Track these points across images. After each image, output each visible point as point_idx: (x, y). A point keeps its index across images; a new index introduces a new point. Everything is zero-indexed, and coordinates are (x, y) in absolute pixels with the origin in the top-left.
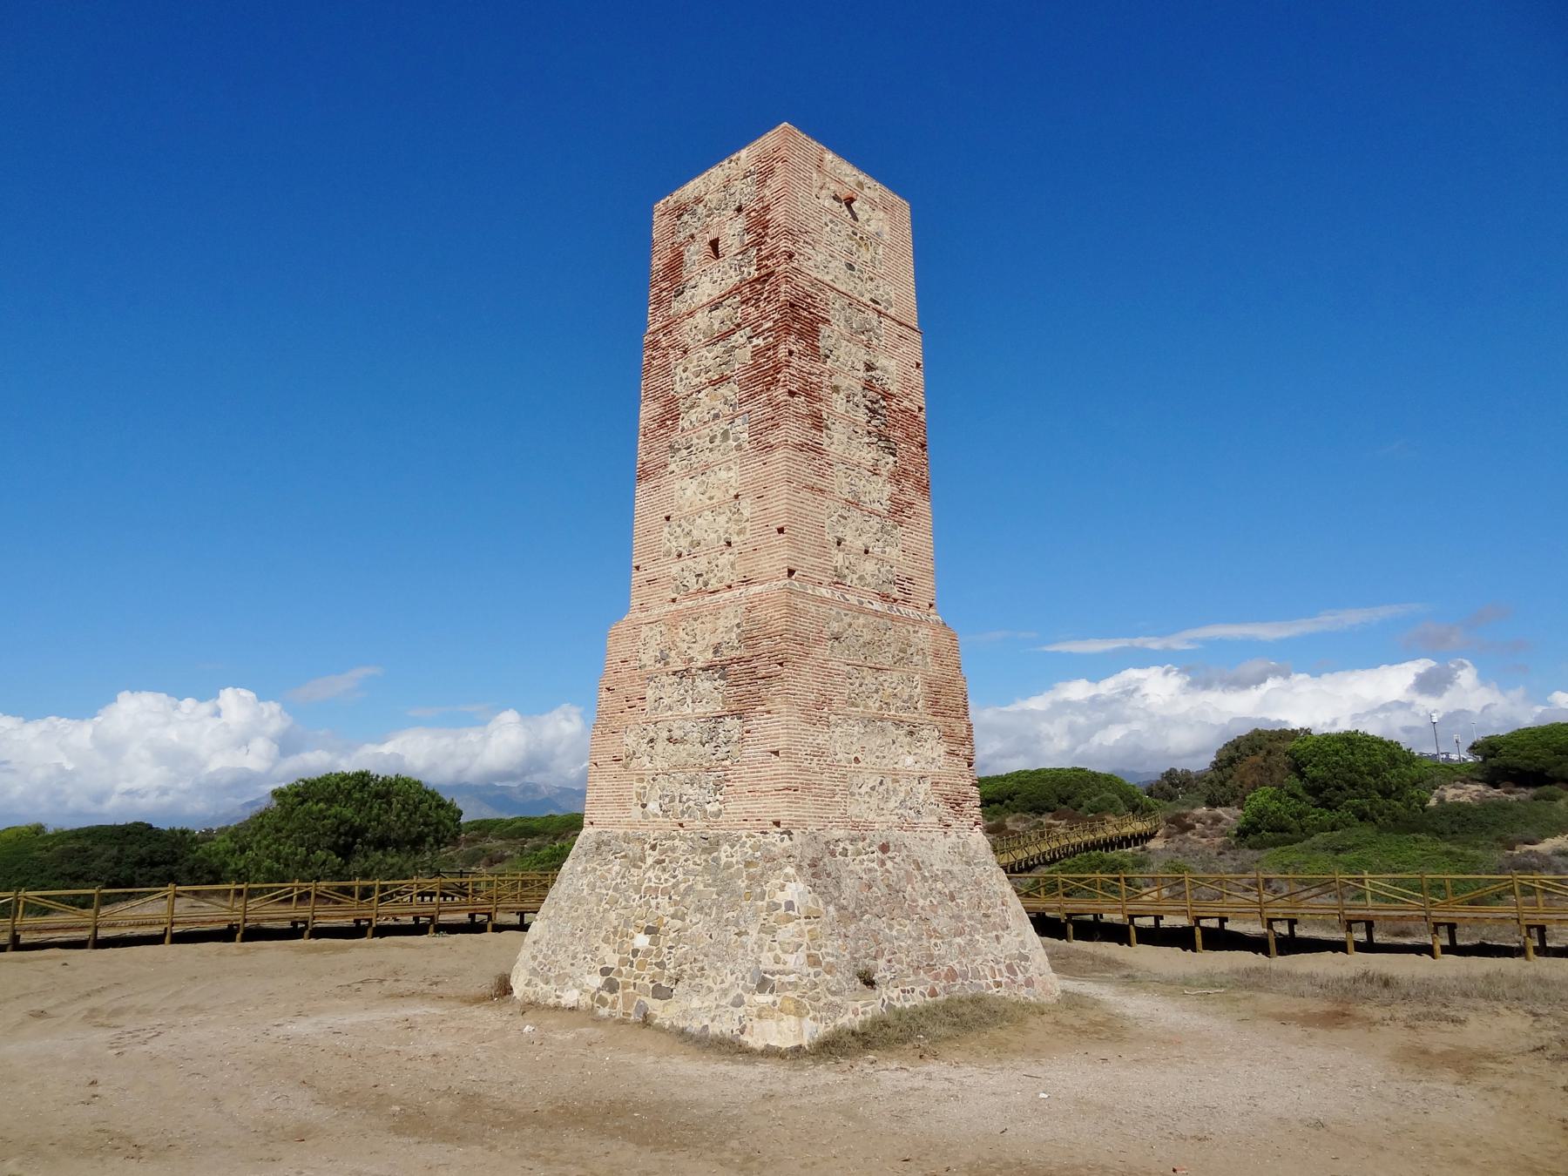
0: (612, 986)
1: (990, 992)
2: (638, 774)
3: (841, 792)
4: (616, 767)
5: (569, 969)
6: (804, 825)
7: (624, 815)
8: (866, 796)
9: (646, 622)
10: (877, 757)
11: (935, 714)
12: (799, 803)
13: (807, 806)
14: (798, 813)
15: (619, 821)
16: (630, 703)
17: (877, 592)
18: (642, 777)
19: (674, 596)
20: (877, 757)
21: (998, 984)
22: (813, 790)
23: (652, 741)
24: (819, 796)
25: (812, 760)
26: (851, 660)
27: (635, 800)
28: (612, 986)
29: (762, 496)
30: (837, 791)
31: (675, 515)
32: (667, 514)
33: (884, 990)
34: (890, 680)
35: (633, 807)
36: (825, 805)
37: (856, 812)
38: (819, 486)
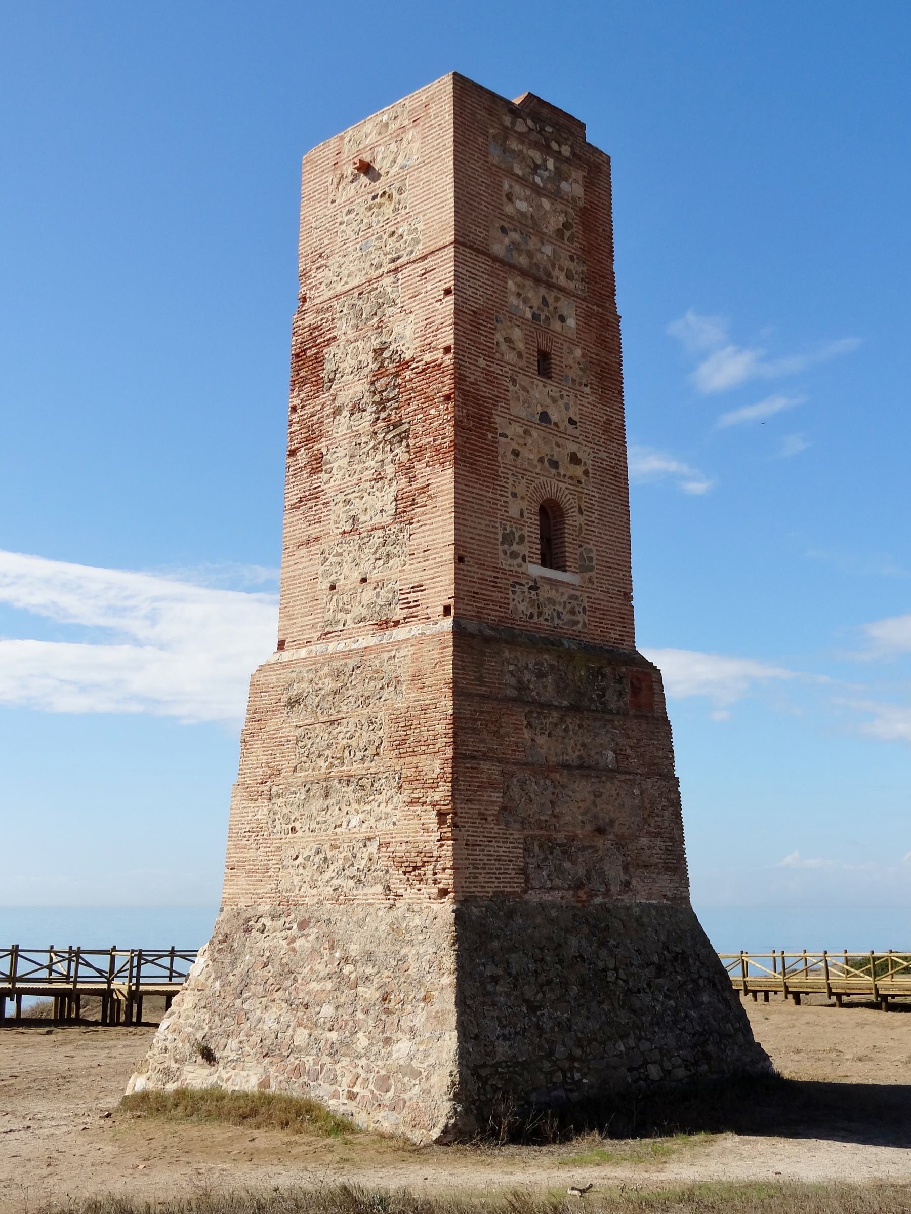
1: (332, 1102)
3: (273, 866)
6: (235, 902)
8: (301, 868)
10: (318, 823)
11: (399, 756)
12: (234, 880)
13: (241, 883)
14: (231, 891)
17: (374, 622)
20: (318, 823)
21: (352, 1096)
22: (249, 867)
24: (253, 872)
25: (250, 836)
26: (303, 720)
30: (270, 865)
33: (220, 1069)
34: (345, 730)
36: (257, 881)
37: (287, 885)
38: (313, 536)
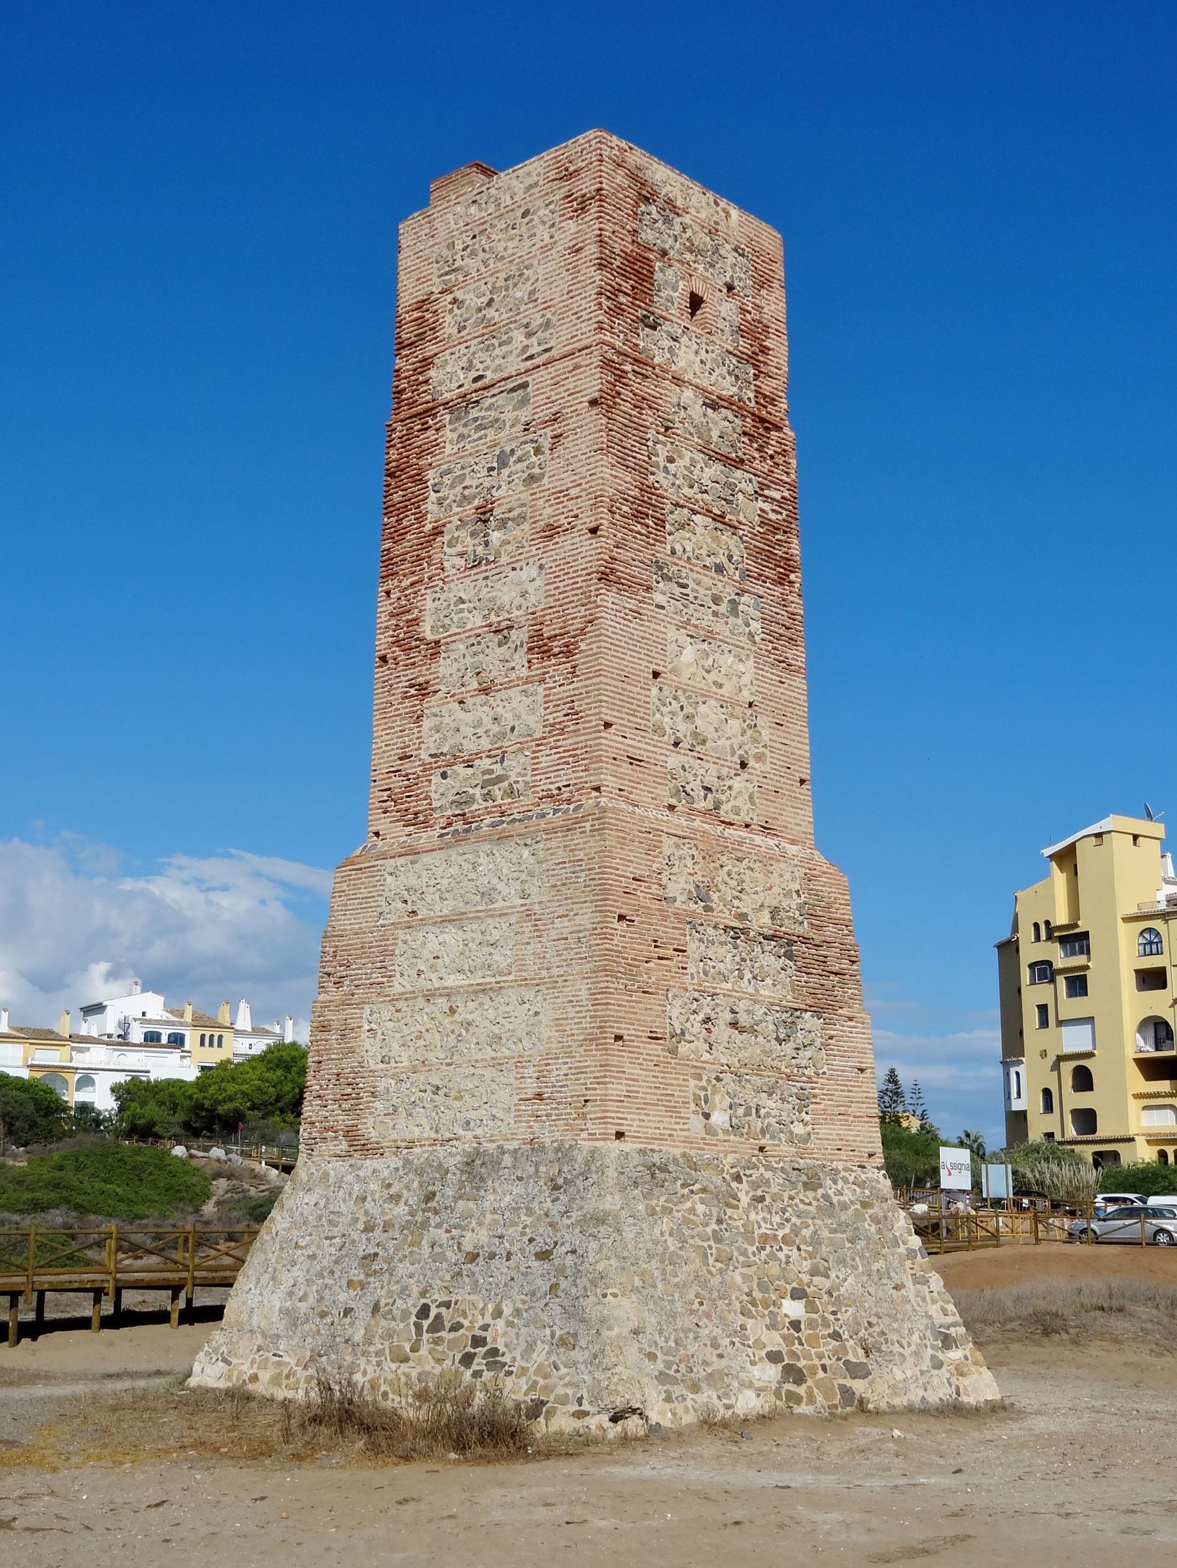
0: (794, 1374)
2: (694, 1067)
4: (656, 1048)
5: (718, 1365)
7: (677, 1127)
9: (670, 831)
15: (670, 1135)
16: (662, 952)
18: (698, 1071)
19: (673, 801)
23: (708, 1020)
27: (692, 1106)
28: (794, 1374)
29: (776, 723)
31: (667, 677)
32: (660, 669)
35: (692, 1116)
